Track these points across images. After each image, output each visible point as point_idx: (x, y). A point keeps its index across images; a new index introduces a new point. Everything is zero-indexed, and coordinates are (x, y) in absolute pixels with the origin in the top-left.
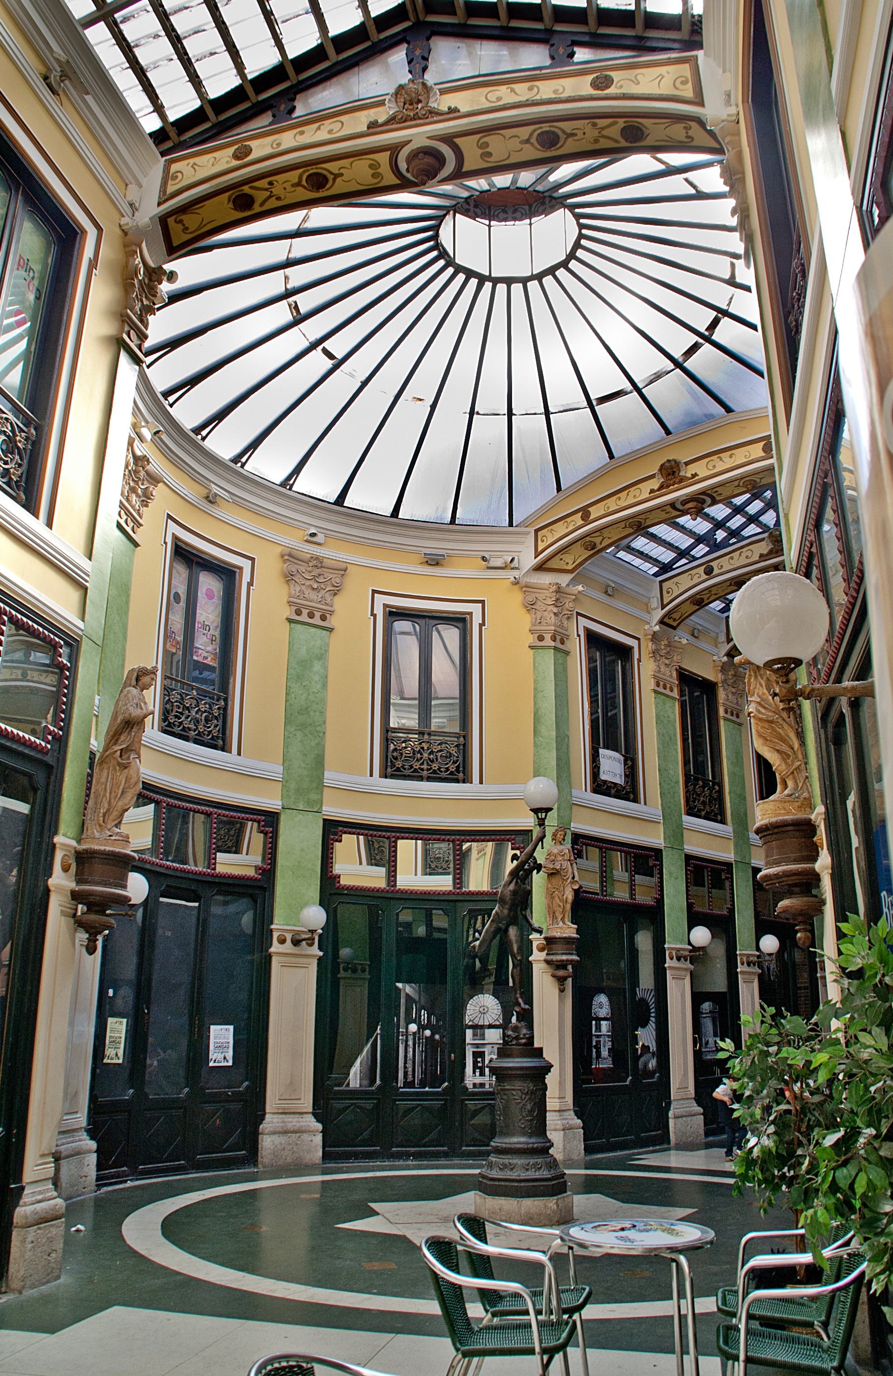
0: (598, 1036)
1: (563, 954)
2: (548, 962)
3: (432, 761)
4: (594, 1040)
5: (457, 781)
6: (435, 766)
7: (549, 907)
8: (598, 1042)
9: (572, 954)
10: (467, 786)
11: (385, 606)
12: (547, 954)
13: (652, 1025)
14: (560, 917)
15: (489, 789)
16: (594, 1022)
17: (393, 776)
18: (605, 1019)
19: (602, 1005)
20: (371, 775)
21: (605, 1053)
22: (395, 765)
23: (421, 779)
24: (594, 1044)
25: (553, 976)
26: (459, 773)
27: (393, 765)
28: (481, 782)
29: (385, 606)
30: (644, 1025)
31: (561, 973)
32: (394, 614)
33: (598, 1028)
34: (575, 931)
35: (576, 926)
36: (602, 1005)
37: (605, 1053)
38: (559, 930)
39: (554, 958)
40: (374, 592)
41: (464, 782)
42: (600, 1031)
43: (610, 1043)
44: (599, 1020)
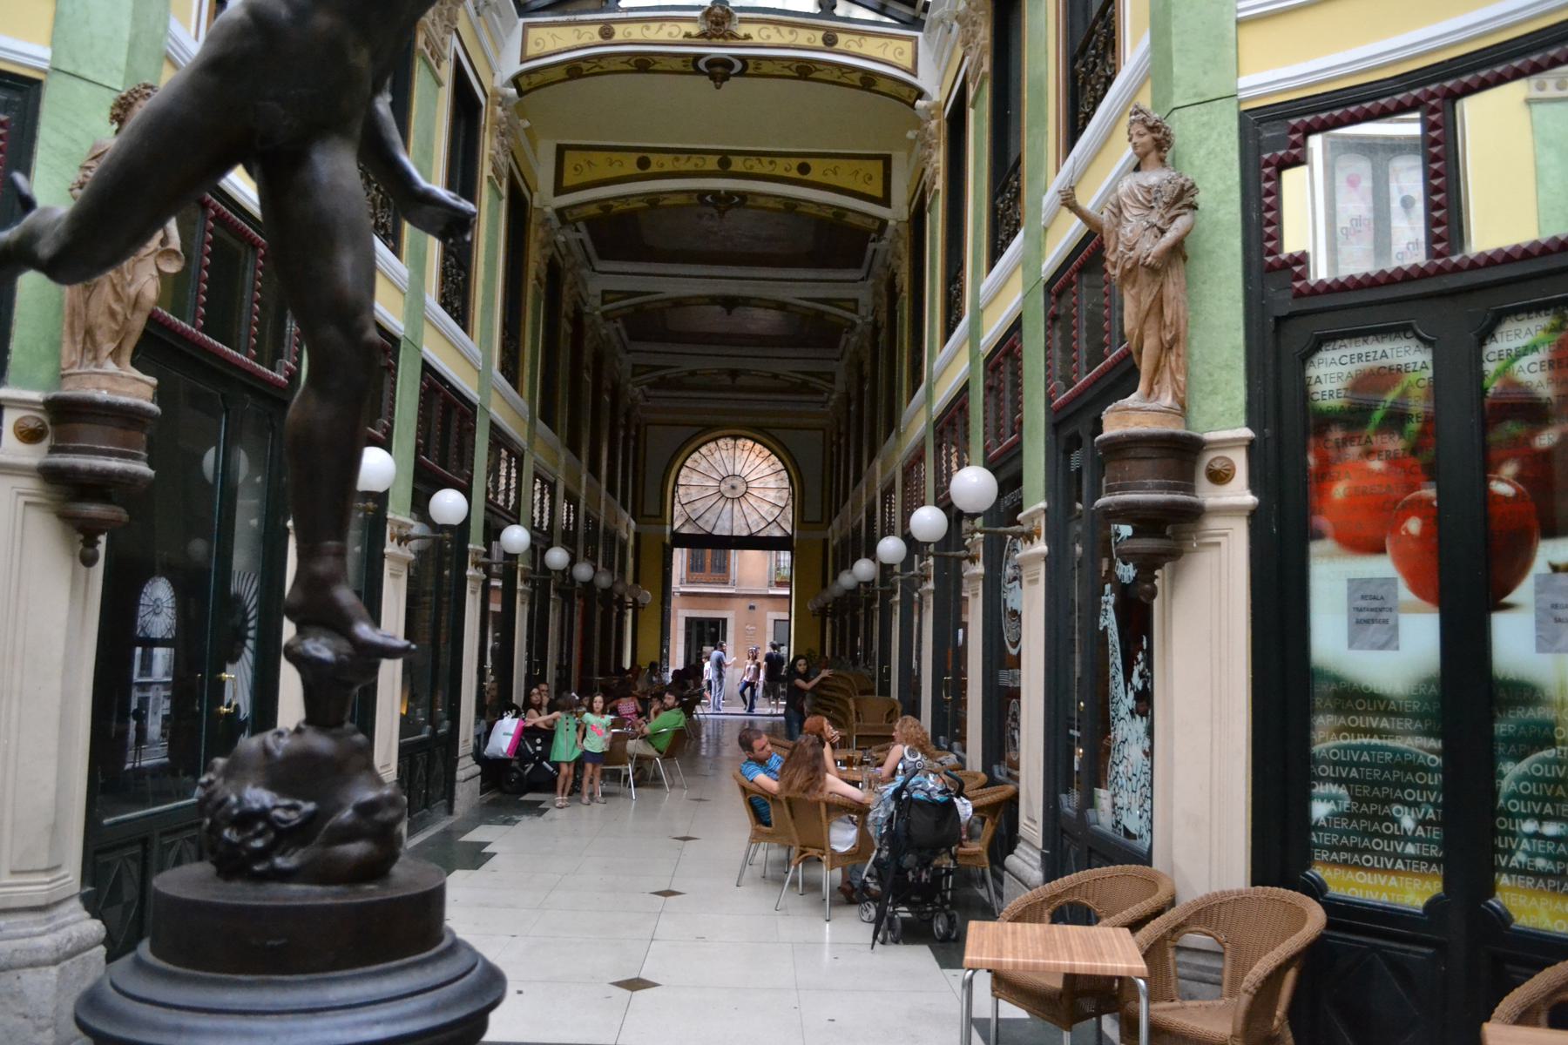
0: (144, 687)
1: (110, 454)
2: (49, 475)
4: (136, 695)
7: (74, 312)
8: (143, 702)
9: (135, 457)
12: (53, 450)
13: (248, 656)
14: (108, 347)
16: (138, 650)
18: (162, 643)
19: (159, 605)
21: (154, 728)
24: (134, 706)
25: (66, 518)
30: (234, 658)
31: (95, 510)
33: (147, 667)
34: (149, 392)
35: (154, 381)
36: (159, 605)
37: (154, 728)
38: (104, 382)
39: (83, 461)
42: (150, 675)
43: (167, 704)
44: (150, 643)
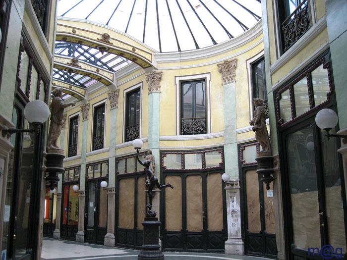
3: (196, 128)
5: (204, 133)
6: (196, 130)
10: (205, 135)
11: (180, 81)
15: (213, 134)
17: (184, 134)
20: (176, 134)
22: (184, 130)
23: (192, 134)
26: (204, 130)
27: (183, 131)
28: (211, 132)
29: (180, 81)
32: (182, 83)
40: (175, 77)
41: (206, 133)
